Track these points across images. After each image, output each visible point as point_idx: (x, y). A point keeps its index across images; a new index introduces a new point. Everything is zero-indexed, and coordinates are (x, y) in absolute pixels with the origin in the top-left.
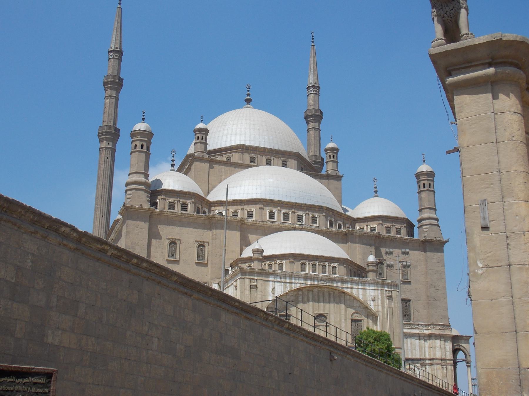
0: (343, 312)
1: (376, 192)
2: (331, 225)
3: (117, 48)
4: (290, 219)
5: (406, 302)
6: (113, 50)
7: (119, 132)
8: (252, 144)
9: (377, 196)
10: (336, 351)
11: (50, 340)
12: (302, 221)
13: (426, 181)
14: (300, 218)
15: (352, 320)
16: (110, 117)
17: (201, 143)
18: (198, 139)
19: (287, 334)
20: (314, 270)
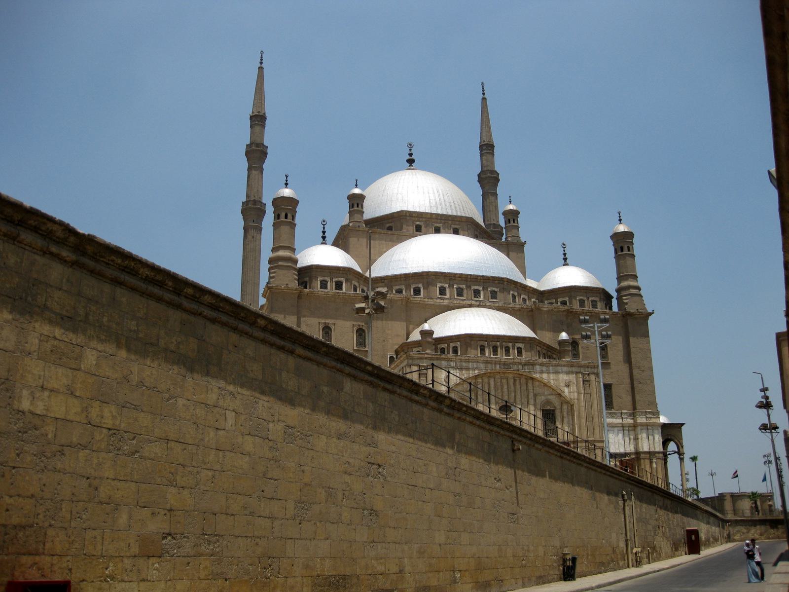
1: (565, 259)
3: (259, 112)
4: (465, 295)
5: (608, 387)
6: (256, 115)
7: (265, 208)
10: (520, 439)
11: (26, 405)
12: (480, 296)
14: (477, 293)
19: (448, 414)
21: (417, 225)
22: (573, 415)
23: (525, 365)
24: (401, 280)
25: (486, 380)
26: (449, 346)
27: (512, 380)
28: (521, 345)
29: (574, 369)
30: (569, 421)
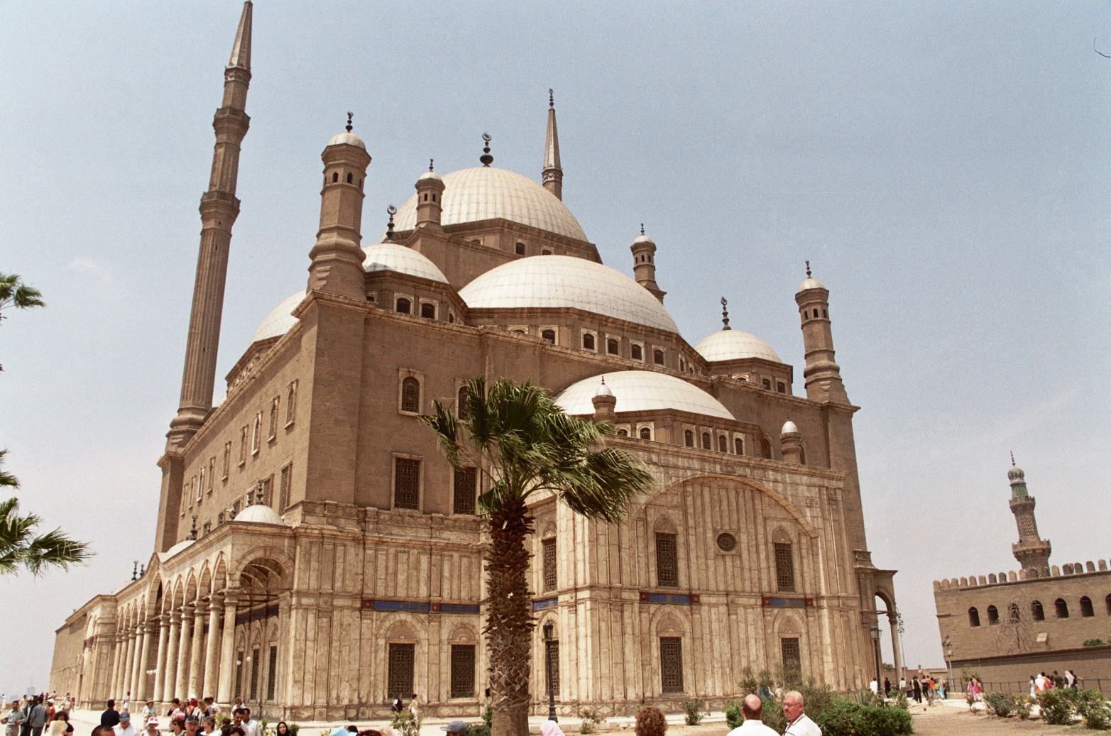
0: (761, 529)
1: (726, 321)
2: (682, 370)
3: (242, 65)
4: (620, 351)
6: (236, 69)
7: (238, 206)
8: (517, 220)
9: (729, 329)
13: (813, 306)
14: (636, 353)
15: (776, 545)
16: (225, 178)
17: (431, 205)
18: (426, 199)
20: (707, 446)
21: (518, 244)
22: (815, 555)
23: (754, 468)
24: (521, 317)
25: (698, 489)
26: (634, 429)
27: (733, 492)
28: (740, 436)
29: (815, 480)
30: (809, 564)
